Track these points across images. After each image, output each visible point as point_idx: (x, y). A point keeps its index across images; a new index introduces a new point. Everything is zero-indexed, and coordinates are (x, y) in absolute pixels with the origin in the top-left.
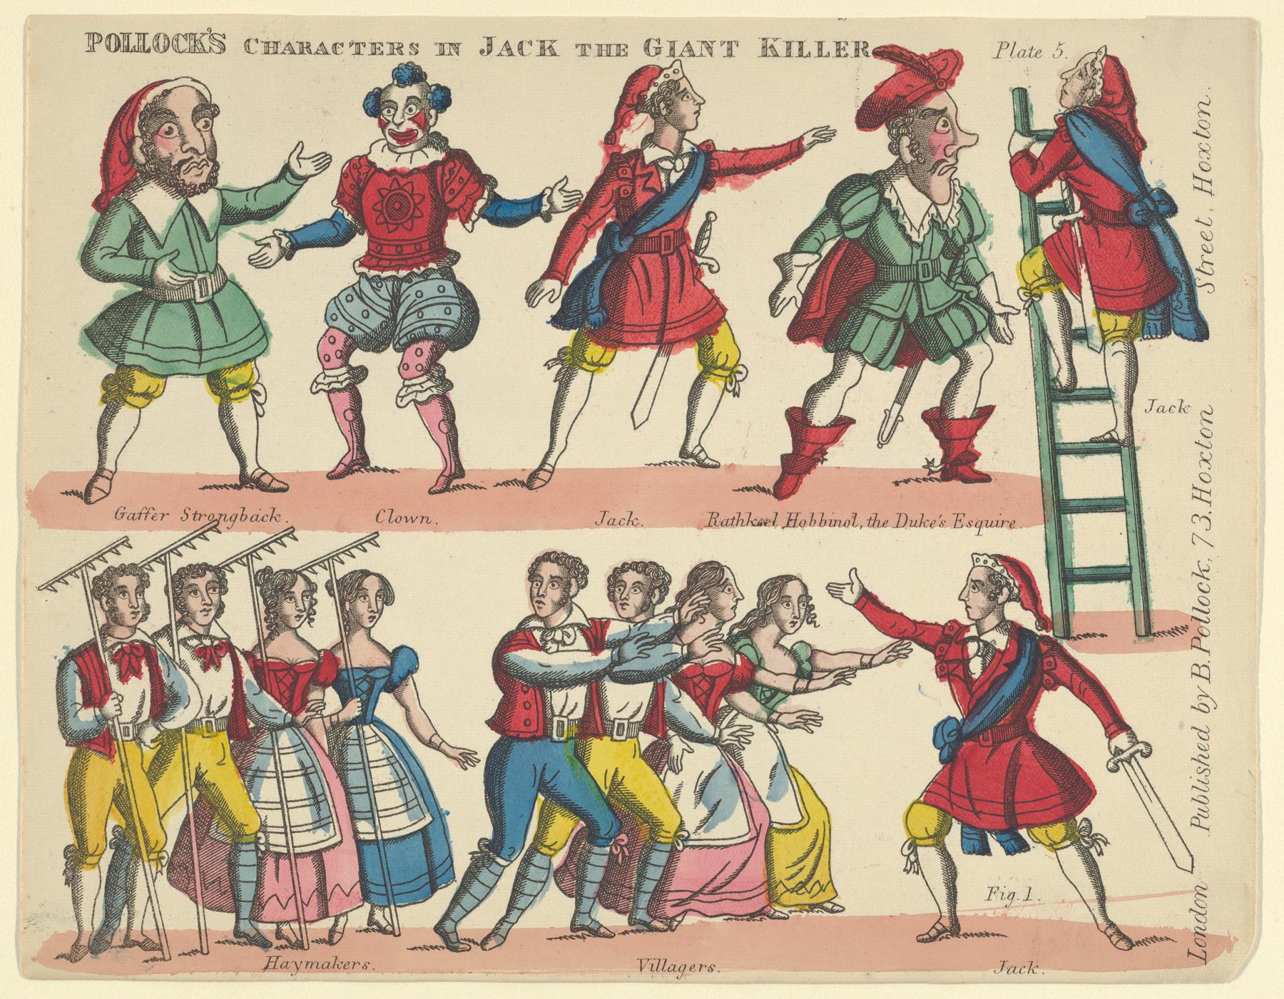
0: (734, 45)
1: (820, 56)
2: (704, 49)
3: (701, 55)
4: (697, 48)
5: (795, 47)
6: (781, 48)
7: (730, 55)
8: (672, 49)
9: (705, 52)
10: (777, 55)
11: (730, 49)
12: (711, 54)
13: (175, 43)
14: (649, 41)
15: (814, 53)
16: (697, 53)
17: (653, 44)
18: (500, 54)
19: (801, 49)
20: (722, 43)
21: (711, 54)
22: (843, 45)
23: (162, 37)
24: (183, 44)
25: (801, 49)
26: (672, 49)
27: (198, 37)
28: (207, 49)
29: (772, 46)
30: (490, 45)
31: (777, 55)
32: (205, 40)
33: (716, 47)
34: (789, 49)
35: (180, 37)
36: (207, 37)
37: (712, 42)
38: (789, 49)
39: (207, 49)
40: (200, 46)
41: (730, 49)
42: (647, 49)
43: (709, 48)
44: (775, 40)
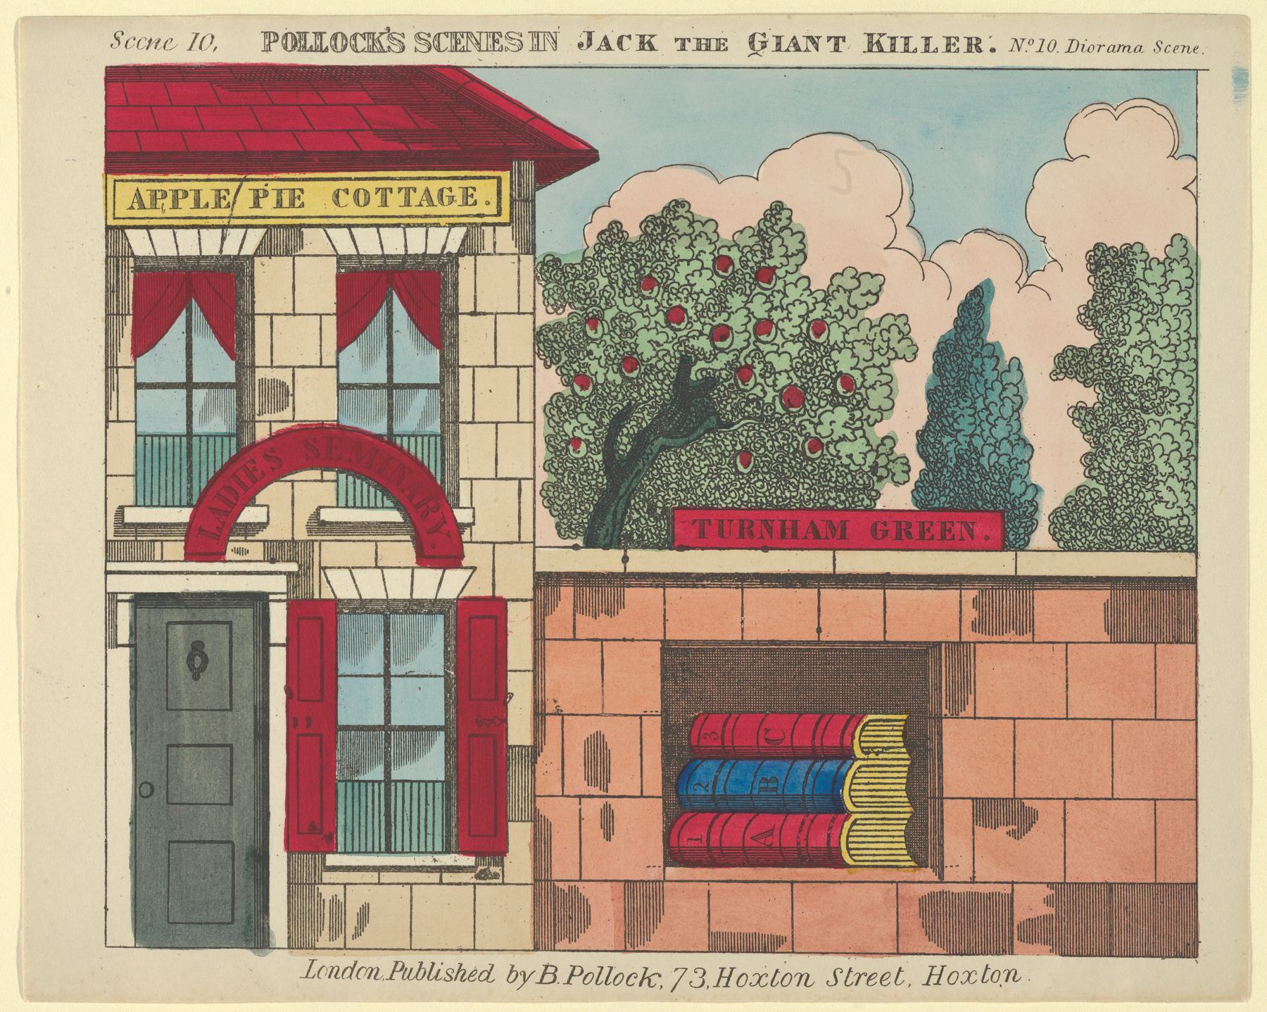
0: (841, 40)
1: (927, 51)
2: (810, 44)
3: (807, 50)
4: (803, 43)
5: (900, 44)
6: (886, 43)
7: (837, 50)
8: (779, 44)
9: (811, 47)
10: (881, 50)
11: (837, 44)
12: (817, 49)
13: (353, 42)
14: (753, 35)
15: (921, 47)
16: (803, 48)
17: (758, 38)
18: (599, 49)
19: (906, 44)
20: (829, 38)
21: (817, 49)
22: (953, 40)
23: (339, 36)
24: (361, 44)
25: (906, 44)
26: (779, 44)
27: (376, 37)
28: (386, 49)
29: (878, 42)
30: (590, 39)
31: (881, 50)
32: (385, 41)
33: (822, 42)
34: (893, 45)
35: (358, 36)
36: (386, 35)
37: (818, 38)
38: (893, 45)
39: (386, 49)
40: (378, 45)
41: (837, 44)
42: (752, 43)
43: (814, 43)
44: (881, 35)
